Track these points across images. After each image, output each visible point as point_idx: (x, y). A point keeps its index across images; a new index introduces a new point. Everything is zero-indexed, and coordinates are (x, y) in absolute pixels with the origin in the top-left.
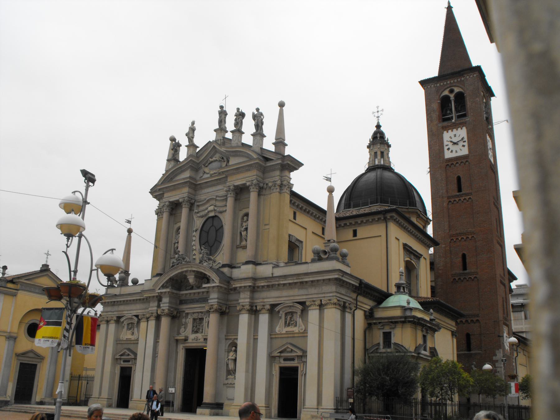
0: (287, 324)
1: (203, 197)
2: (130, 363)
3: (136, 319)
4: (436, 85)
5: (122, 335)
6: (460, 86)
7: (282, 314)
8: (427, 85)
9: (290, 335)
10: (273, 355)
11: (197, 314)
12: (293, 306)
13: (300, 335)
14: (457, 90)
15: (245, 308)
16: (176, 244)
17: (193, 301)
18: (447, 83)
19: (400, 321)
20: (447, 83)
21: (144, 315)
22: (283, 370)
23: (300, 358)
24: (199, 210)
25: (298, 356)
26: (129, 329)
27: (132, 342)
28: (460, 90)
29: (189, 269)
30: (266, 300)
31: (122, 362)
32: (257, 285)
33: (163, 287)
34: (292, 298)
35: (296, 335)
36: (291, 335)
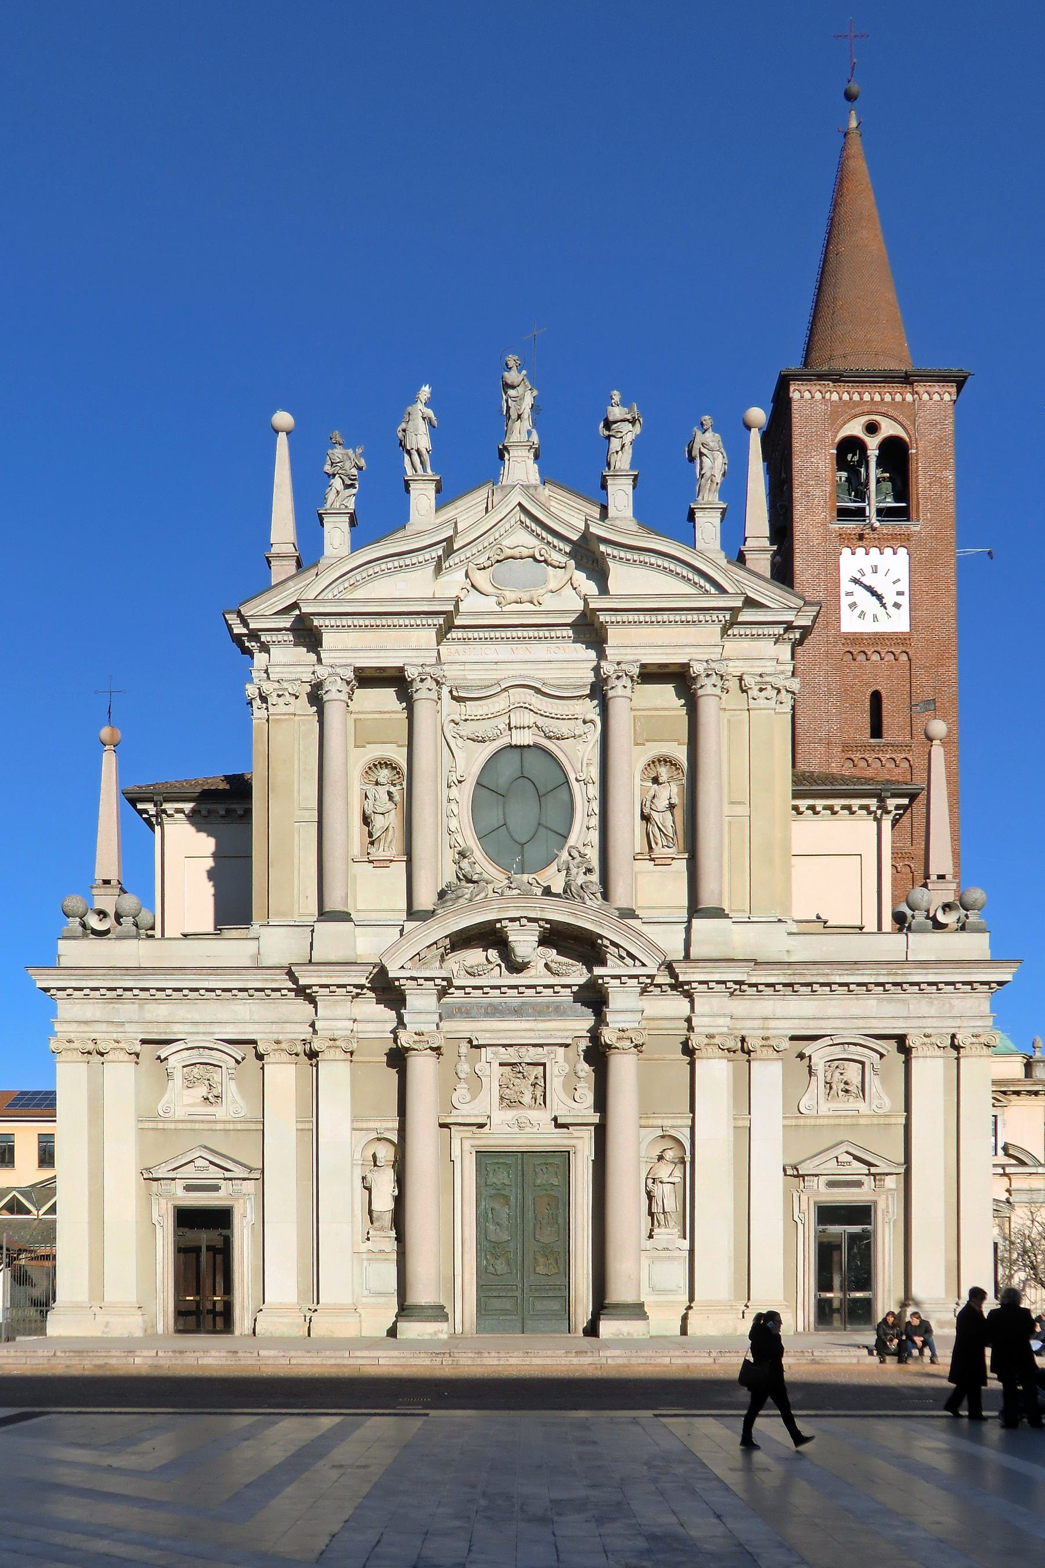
0: (832, 1092)
1: (475, 675)
2: (221, 1193)
3: (237, 1051)
4: (828, 395)
5: (163, 1101)
6: (901, 418)
7: (819, 1063)
8: (802, 388)
9: (842, 1121)
10: (800, 1173)
11: (523, 1049)
12: (855, 1044)
13: (875, 1121)
14: (888, 429)
15: (716, 1041)
16: (379, 822)
17: (493, 1011)
18: (861, 399)
19: (1028, 1091)
20: (861, 399)
21: (278, 1042)
22: (827, 1214)
23: (880, 1180)
24: (467, 717)
25: (874, 1175)
26: (190, 1083)
27: (219, 1127)
28: (900, 432)
29: (532, 915)
30: (772, 1024)
31: (180, 1192)
32: (754, 980)
33: (418, 957)
34: (861, 1023)
35: (862, 1121)
36: (848, 1121)
